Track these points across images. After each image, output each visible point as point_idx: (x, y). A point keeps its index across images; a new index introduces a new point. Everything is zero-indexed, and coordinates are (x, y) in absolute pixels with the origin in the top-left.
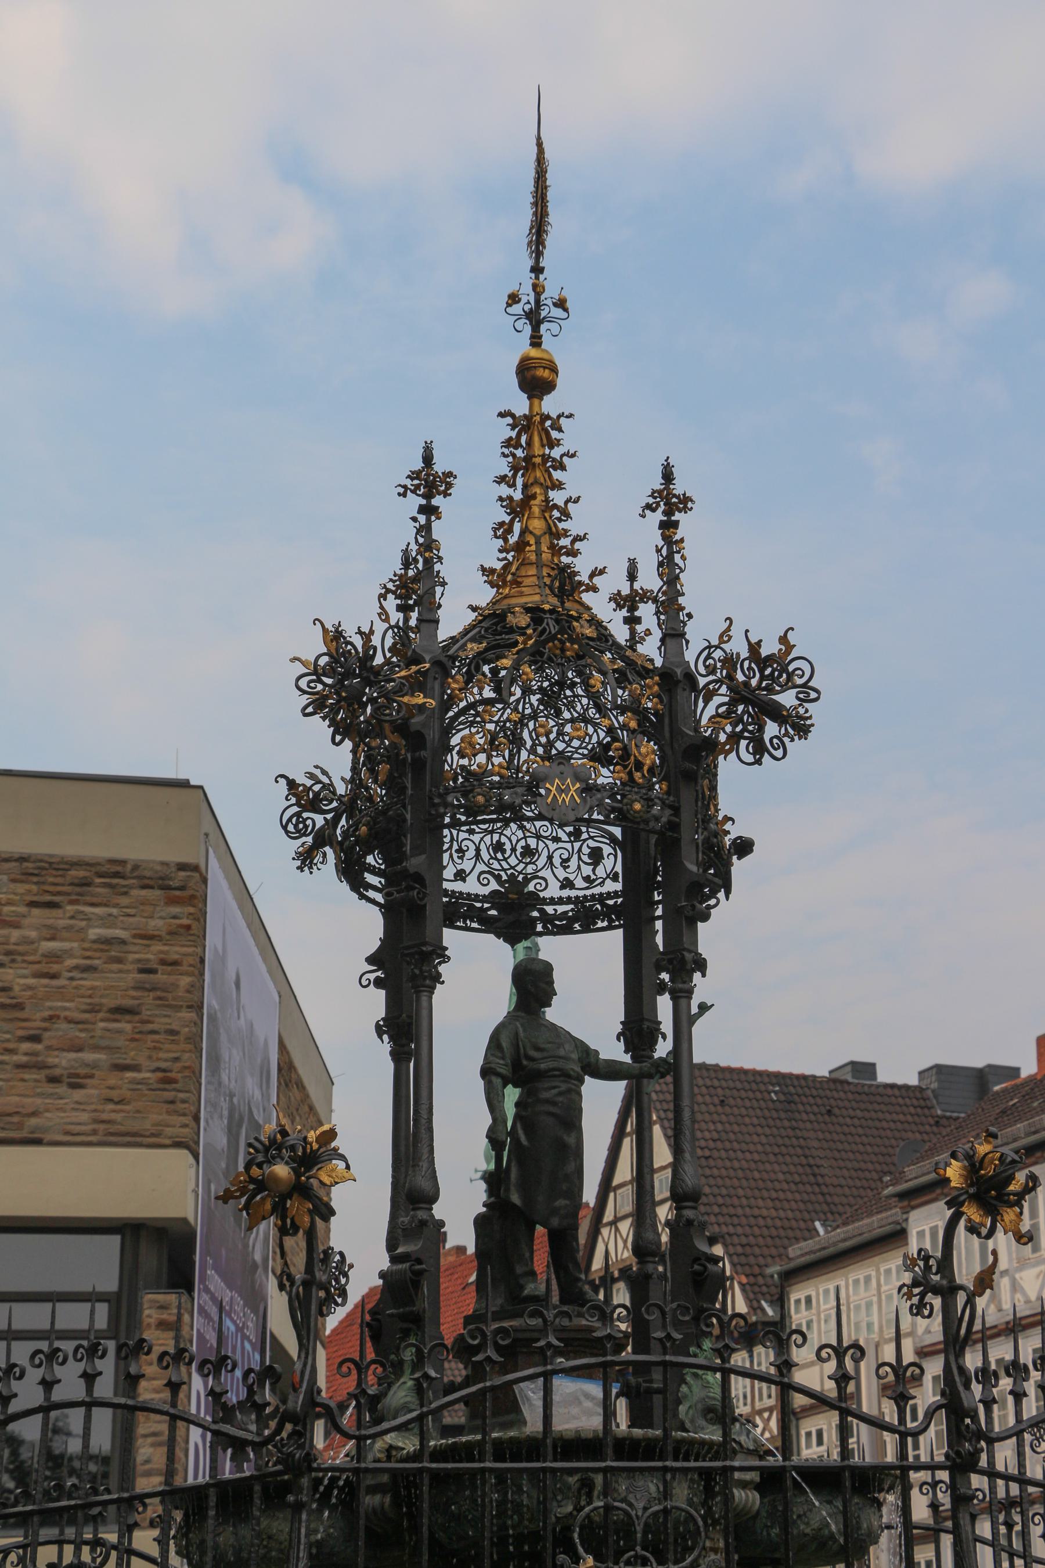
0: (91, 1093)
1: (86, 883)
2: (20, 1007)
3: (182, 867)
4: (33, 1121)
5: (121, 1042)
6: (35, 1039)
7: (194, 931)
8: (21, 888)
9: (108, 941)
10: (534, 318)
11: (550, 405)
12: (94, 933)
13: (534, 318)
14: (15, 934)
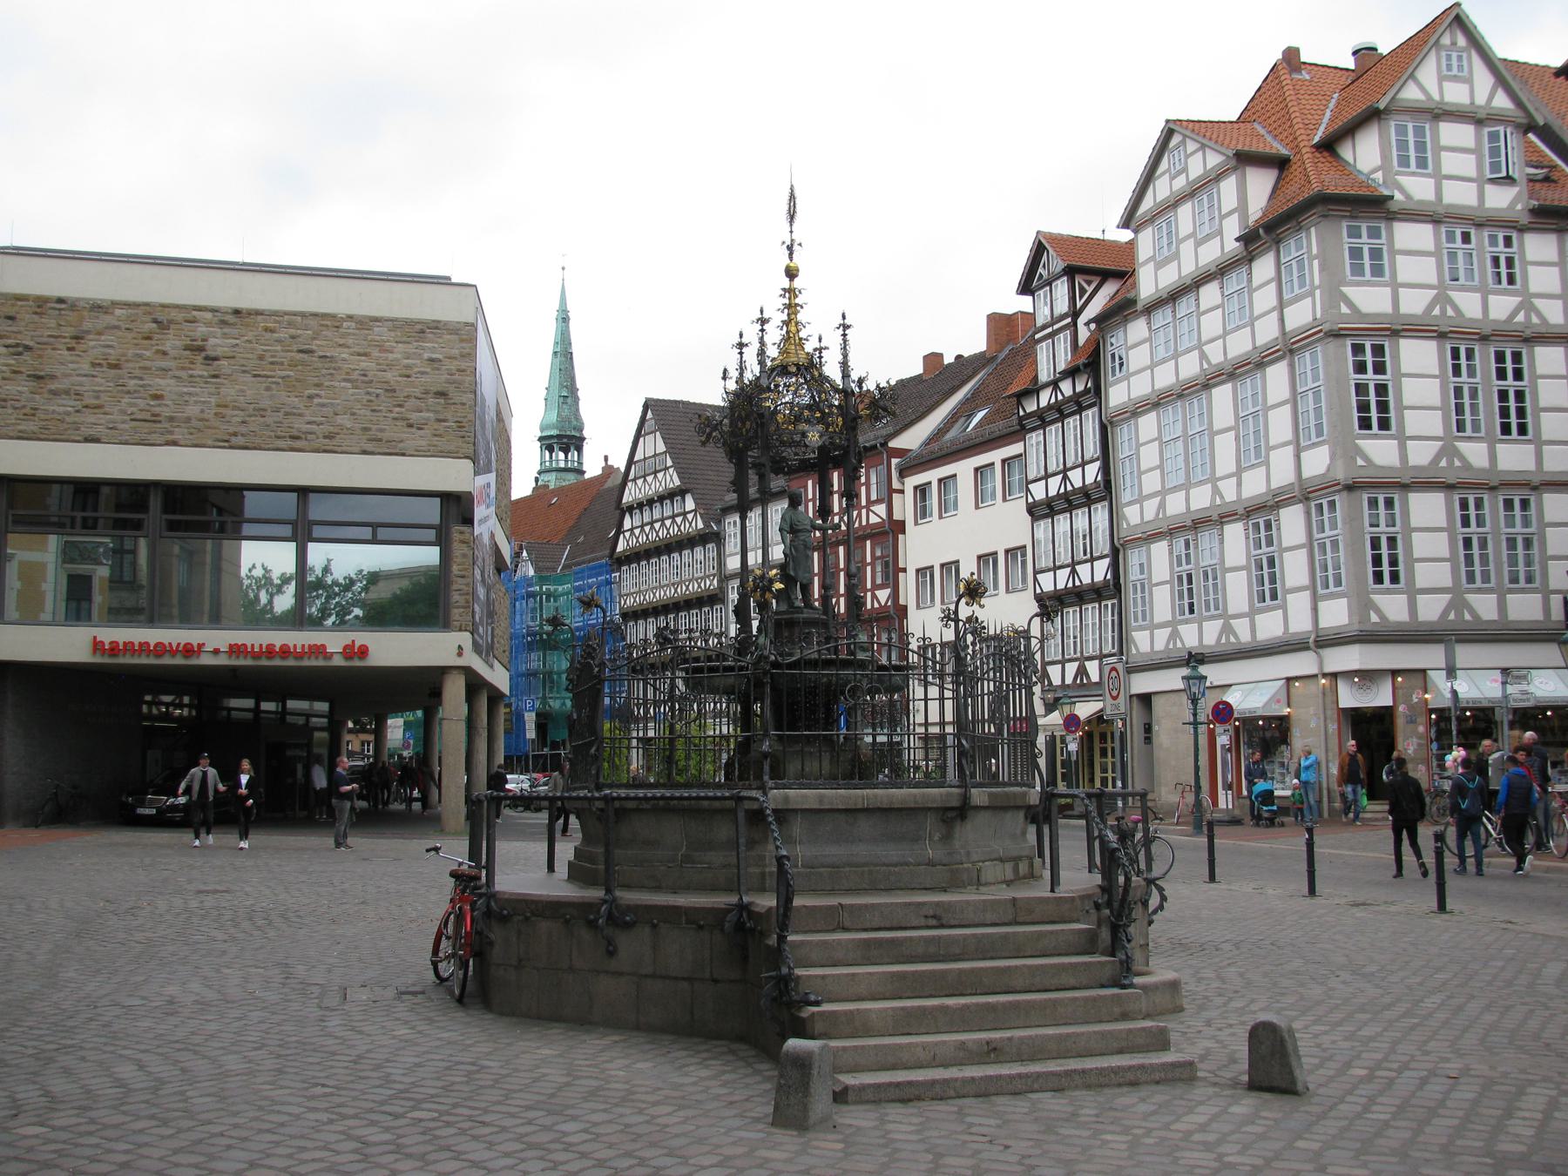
0: (427, 432)
1: (423, 332)
3: (467, 324)
5: (439, 408)
7: (471, 356)
9: (432, 360)
10: (790, 248)
11: (797, 283)
12: (426, 356)
13: (790, 248)
14: (391, 356)
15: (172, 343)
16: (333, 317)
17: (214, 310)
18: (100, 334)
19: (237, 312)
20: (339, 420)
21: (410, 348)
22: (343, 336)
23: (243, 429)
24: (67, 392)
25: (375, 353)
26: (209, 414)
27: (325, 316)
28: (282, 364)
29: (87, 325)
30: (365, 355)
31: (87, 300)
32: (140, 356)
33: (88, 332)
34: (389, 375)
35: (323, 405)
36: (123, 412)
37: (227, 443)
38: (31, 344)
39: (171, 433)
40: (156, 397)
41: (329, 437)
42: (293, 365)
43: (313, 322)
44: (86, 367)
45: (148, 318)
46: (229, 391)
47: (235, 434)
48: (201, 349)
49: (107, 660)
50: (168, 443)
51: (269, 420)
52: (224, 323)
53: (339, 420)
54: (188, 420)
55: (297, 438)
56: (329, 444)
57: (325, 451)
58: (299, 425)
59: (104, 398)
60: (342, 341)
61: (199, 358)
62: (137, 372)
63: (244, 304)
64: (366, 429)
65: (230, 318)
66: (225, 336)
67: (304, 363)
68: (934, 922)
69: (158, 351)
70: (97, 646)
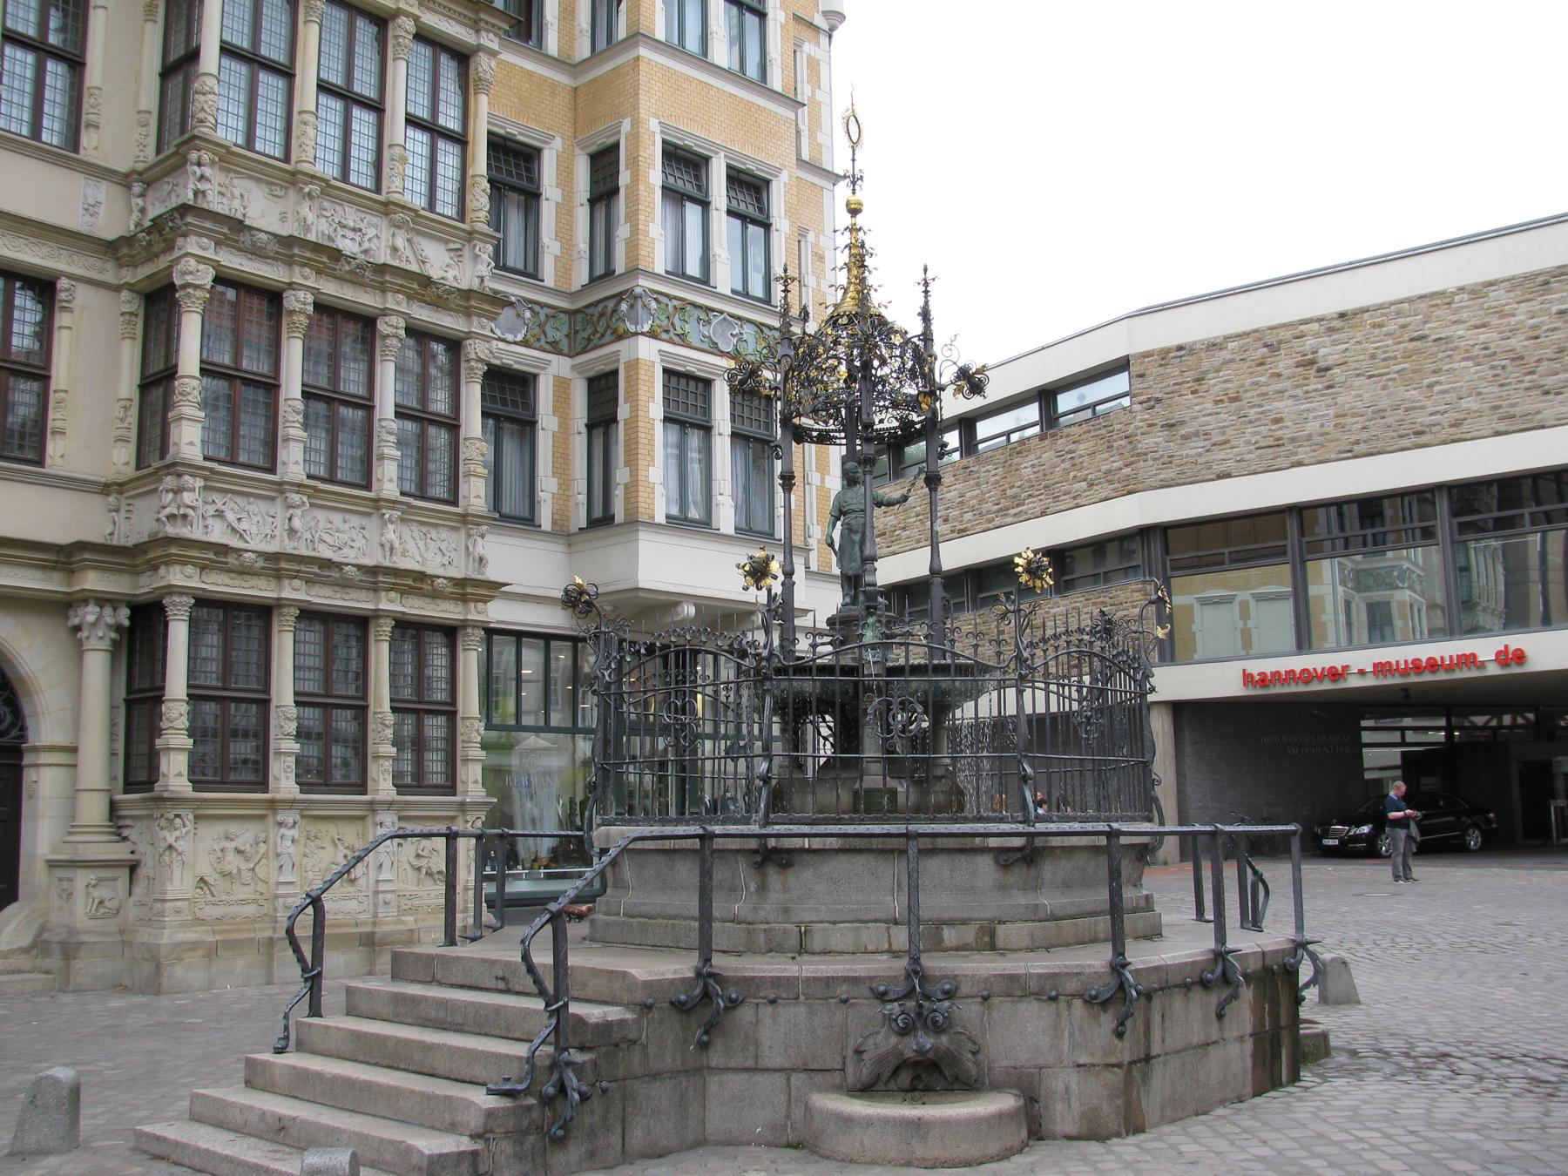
1: (1546, 283)
2: (1522, 358)
4: (1539, 417)
6: (1530, 373)
8: (1512, 295)
12: (1554, 309)
14: (1513, 320)
15: (1284, 363)
16: (1443, 293)
17: (1319, 320)
18: (1218, 371)
19: (1342, 315)
20: (1464, 404)
21: (1535, 305)
22: (1457, 311)
23: (1364, 435)
24: (1196, 434)
25: (1495, 321)
26: (1329, 427)
27: (1433, 295)
28: (1395, 358)
29: (1205, 366)
30: (1484, 326)
31: (1201, 342)
32: (1257, 383)
33: (1207, 372)
34: (1514, 342)
35: (1445, 392)
36: (1248, 443)
37: (1350, 453)
38: (1160, 396)
39: (1296, 454)
40: (1277, 421)
41: (1456, 424)
42: (1407, 356)
43: (1422, 306)
44: (1210, 405)
45: (1260, 344)
46: (1346, 399)
47: (1357, 443)
48: (1312, 362)
49: (1260, 692)
50: (1294, 465)
51: (1390, 420)
52: (1331, 330)
53: (1464, 404)
54: (1309, 437)
55: (1422, 433)
56: (1457, 433)
57: (1453, 441)
58: (1423, 419)
59: (1230, 432)
60: (1455, 318)
61: (1313, 372)
62: (1256, 401)
63: (1348, 306)
64: (1496, 408)
65: (1336, 324)
66: (1335, 343)
67: (1418, 351)
68: (502, 985)
69: (1272, 375)
70: (1247, 678)
